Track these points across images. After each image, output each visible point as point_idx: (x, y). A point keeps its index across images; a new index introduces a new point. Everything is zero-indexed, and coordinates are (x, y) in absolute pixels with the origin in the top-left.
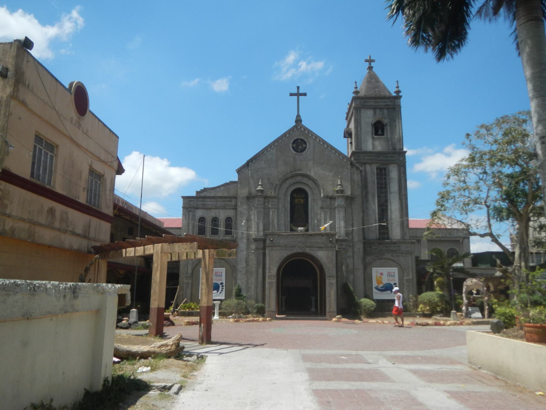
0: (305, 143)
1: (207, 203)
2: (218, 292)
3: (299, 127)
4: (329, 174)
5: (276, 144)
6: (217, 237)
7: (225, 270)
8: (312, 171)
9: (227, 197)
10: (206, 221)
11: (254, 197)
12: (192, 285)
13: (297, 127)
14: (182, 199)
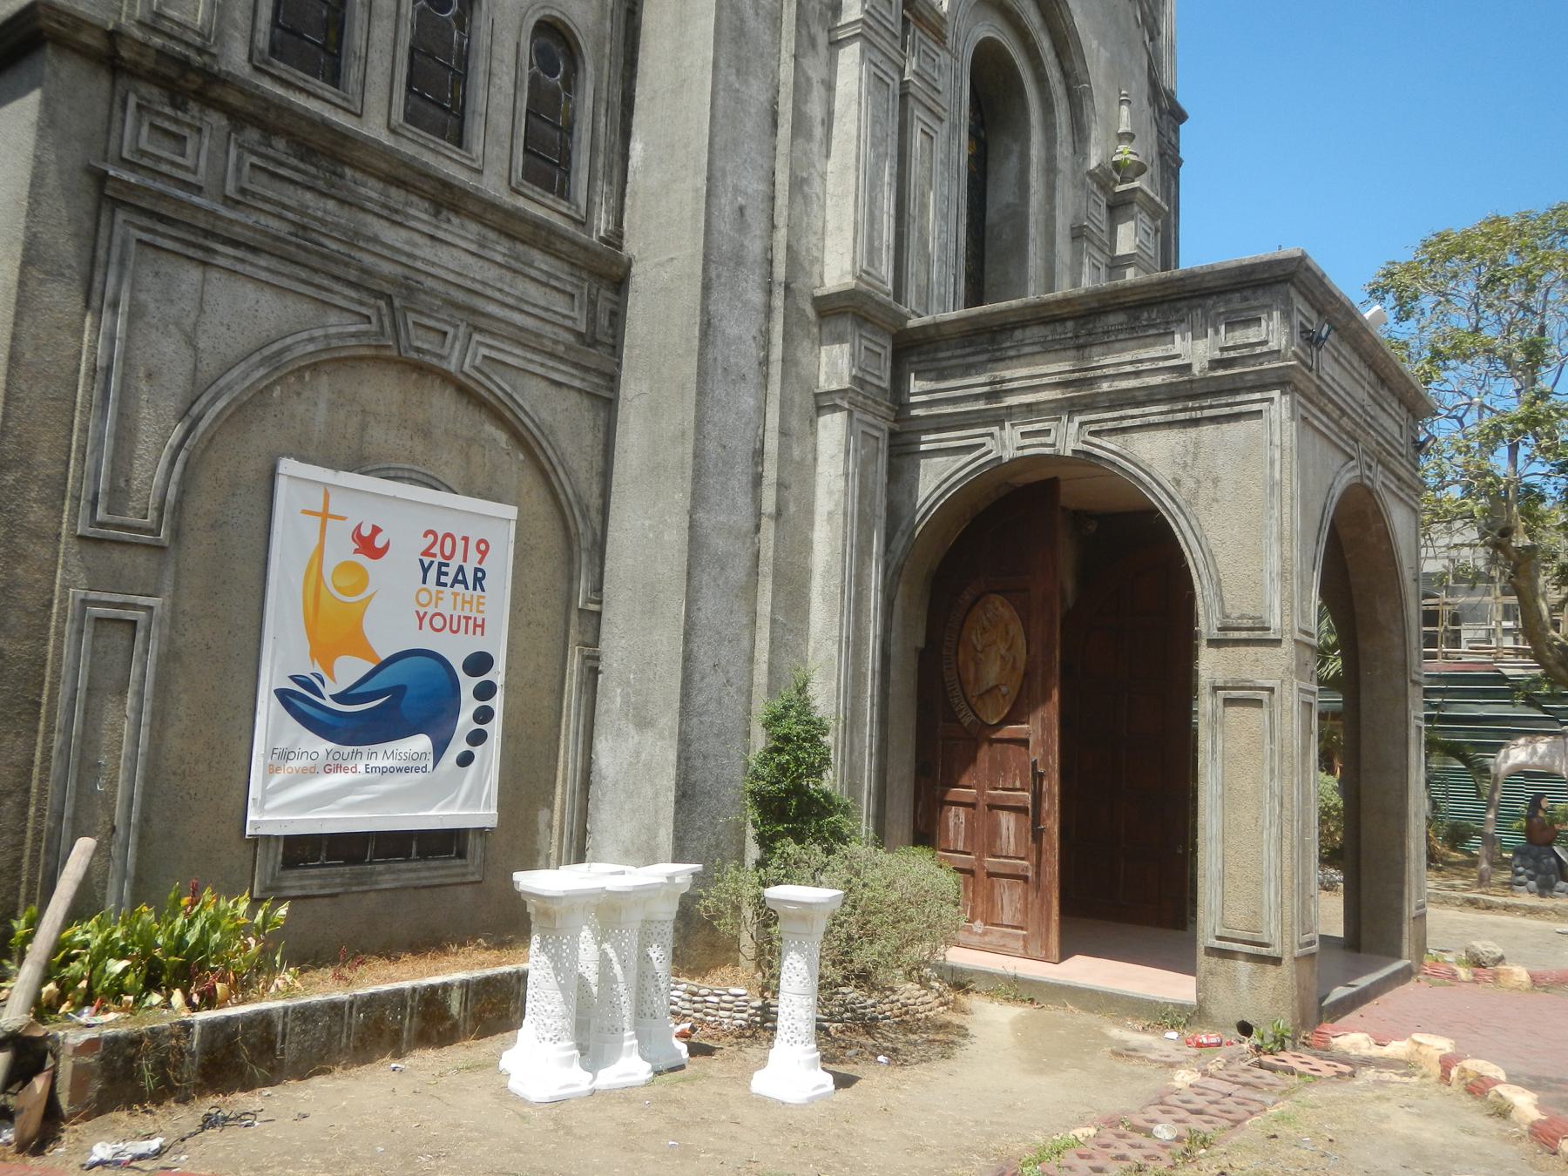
2: (439, 750)
7: (513, 526)
12: (170, 657)
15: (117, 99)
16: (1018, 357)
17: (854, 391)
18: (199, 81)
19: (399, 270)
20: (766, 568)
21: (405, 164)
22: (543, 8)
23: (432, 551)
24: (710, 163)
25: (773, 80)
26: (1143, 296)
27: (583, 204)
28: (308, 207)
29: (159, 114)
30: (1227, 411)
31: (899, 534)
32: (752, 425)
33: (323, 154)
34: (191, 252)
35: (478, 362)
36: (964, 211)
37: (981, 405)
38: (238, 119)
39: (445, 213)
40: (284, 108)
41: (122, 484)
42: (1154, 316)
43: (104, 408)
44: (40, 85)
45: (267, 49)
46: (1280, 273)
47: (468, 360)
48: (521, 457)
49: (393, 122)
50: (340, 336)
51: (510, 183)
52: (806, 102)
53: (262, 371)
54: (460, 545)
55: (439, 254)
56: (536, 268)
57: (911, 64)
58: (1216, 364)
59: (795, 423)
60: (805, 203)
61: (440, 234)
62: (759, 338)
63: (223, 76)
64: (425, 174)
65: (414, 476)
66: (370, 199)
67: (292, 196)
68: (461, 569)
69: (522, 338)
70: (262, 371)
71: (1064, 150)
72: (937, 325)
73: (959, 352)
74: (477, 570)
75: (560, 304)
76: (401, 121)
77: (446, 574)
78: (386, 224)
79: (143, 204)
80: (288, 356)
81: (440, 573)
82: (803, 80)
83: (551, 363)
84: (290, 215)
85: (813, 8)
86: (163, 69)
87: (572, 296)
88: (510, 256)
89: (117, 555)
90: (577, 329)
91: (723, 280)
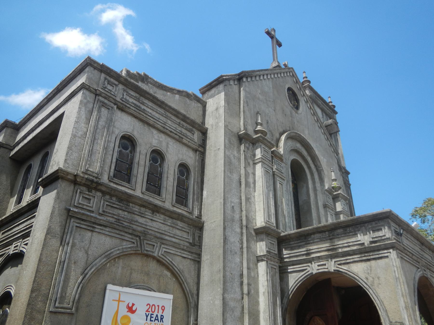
1: (145, 108)
7: (172, 301)
9: (188, 118)
10: (138, 150)
11: (254, 143)
15: (75, 191)
16: (314, 243)
17: (267, 255)
18: (95, 185)
19: (143, 229)
20: (246, 311)
21: (145, 201)
22: (181, 161)
23: (149, 310)
24: (224, 196)
25: (239, 174)
26: (347, 224)
27: (191, 208)
28: (120, 214)
29: (85, 194)
30: (377, 256)
31: (285, 298)
32: (239, 267)
33: (125, 200)
34: (89, 228)
35: (163, 253)
36: (293, 202)
37: (304, 257)
38: (104, 193)
39: (155, 213)
40: (116, 190)
41: (64, 295)
42: (351, 229)
43: (62, 273)
44: (56, 189)
45: (113, 176)
46: (385, 216)
47: (160, 252)
48: (174, 280)
49: (143, 191)
50: (126, 248)
51: (172, 204)
52: (248, 178)
53: (105, 259)
54: (157, 308)
55: (153, 224)
56: (178, 226)
57: (275, 167)
58: (372, 242)
59: (251, 265)
60: (250, 204)
61: (154, 219)
62: (240, 241)
63: (101, 183)
64: (150, 203)
65: (144, 287)
66: (136, 211)
67: (116, 212)
68: (157, 316)
69: (175, 245)
70: (105, 259)
71: (318, 185)
72: (289, 235)
73: (296, 242)
74: (161, 316)
75: (185, 235)
76: (145, 191)
77: (153, 317)
78: (140, 217)
79: (78, 217)
80: (112, 255)
81: (151, 317)
82: (247, 173)
83: (182, 252)
84: (115, 217)
85: (248, 156)
86: (87, 183)
87: (188, 233)
88: (171, 223)
89: (60, 317)
90: (189, 241)
91: (229, 226)
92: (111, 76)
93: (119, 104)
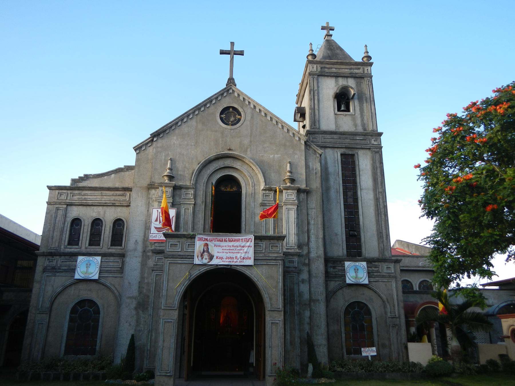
0: (240, 114)
3: (231, 91)
4: (274, 156)
5: (197, 112)
6: (99, 250)
8: (249, 153)
9: (118, 188)
12: (48, 327)
13: (228, 90)
14: (48, 191)
67: (68, 263)
75: (116, 264)
92: (62, 189)
93: (68, 203)
